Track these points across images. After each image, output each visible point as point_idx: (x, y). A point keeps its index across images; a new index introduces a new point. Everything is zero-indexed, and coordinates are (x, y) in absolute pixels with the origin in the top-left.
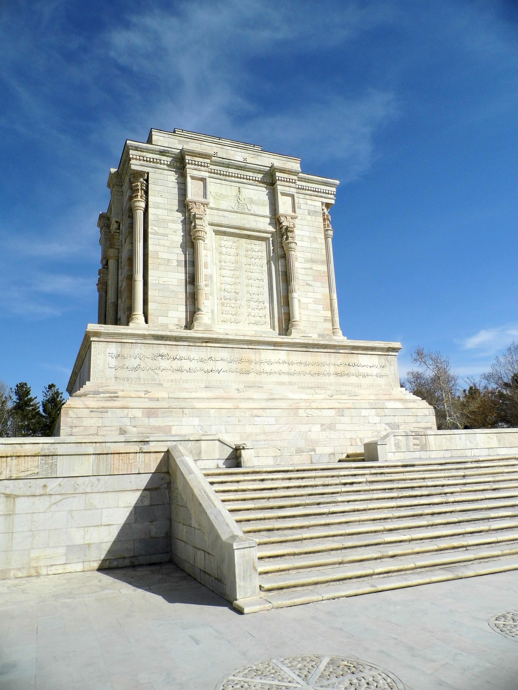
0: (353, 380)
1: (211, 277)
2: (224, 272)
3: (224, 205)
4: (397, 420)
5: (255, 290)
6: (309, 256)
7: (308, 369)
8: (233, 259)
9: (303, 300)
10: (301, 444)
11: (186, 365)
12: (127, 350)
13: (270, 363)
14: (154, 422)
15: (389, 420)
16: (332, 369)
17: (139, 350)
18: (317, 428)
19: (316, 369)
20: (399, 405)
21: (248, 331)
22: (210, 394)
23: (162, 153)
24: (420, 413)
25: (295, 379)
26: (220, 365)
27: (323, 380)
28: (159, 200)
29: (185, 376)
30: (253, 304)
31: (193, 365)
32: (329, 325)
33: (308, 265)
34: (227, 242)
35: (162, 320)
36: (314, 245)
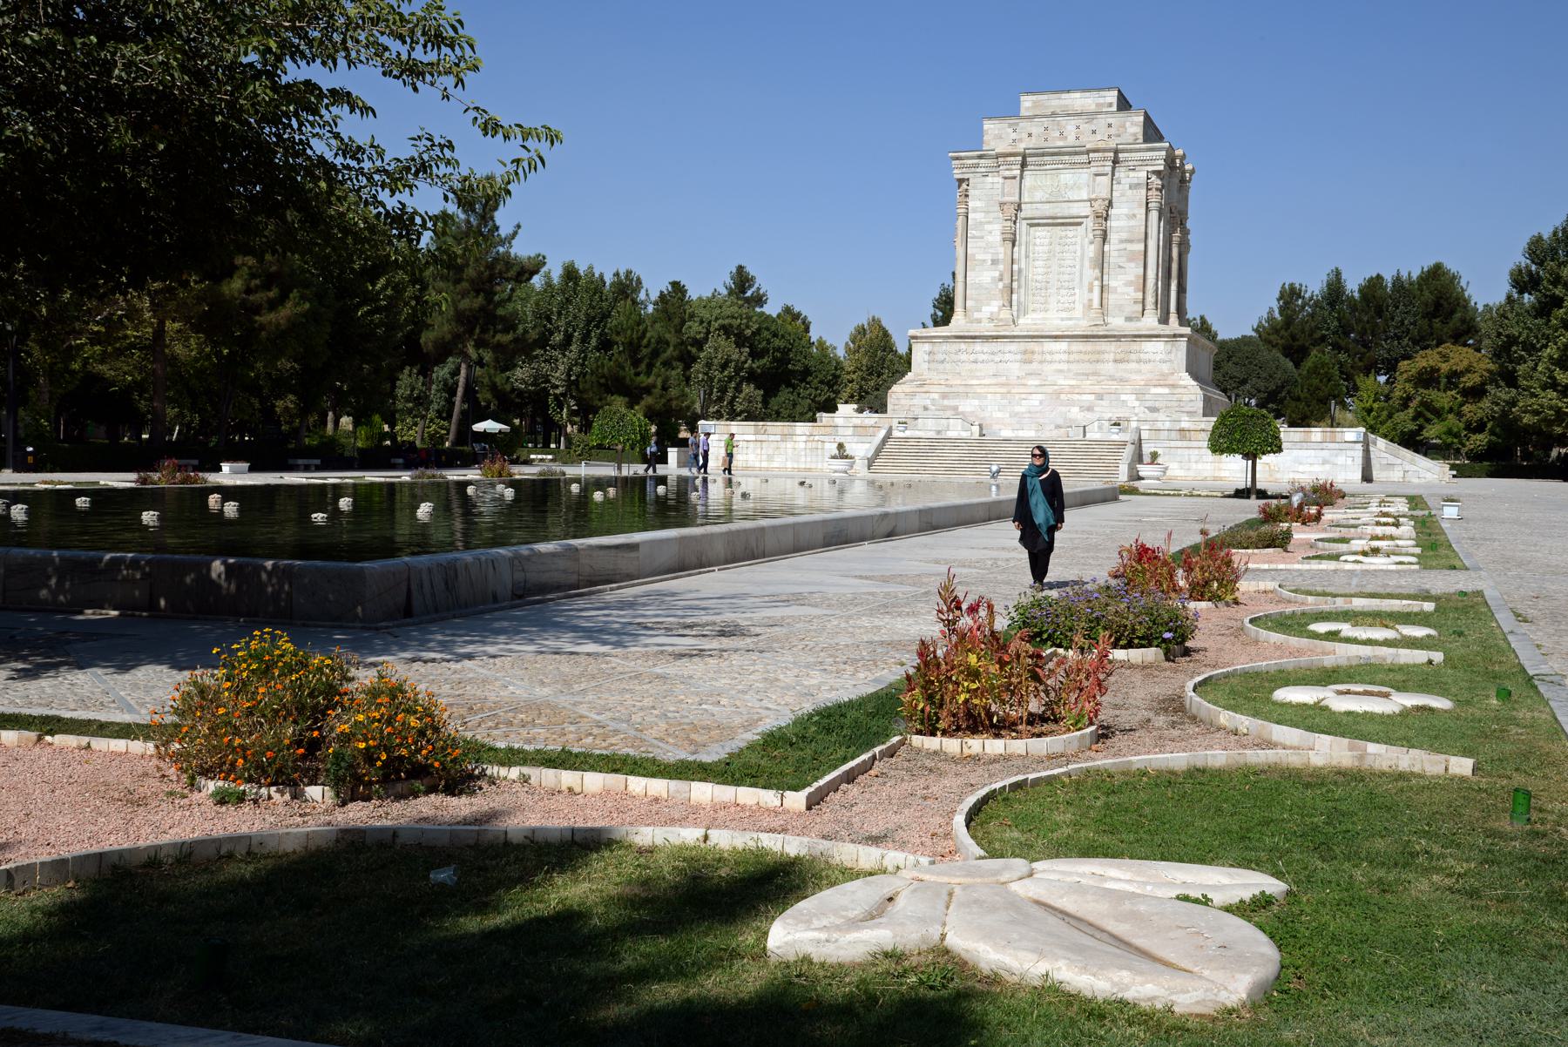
0: (1133, 366)
1: (1020, 271)
2: (1037, 263)
3: (1039, 196)
4: (1157, 405)
5: (1066, 277)
6: (1124, 236)
7: (1087, 357)
8: (1046, 248)
9: (1113, 284)
10: (1060, 421)
11: (981, 357)
12: (937, 348)
13: (1051, 353)
14: (946, 402)
15: (1149, 404)
16: (1111, 357)
17: (945, 347)
18: (1075, 410)
19: (1096, 357)
20: (1166, 391)
21: (1053, 320)
22: (994, 381)
23: (980, 157)
24: (1185, 398)
25: (1073, 367)
26: (1007, 357)
27: (1100, 366)
28: (978, 204)
29: (980, 366)
30: (1063, 292)
31: (985, 357)
32: (1140, 307)
33: (1123, 246)
34: (1040, 232)
35: (976, 315)
36: (1132, 223)
